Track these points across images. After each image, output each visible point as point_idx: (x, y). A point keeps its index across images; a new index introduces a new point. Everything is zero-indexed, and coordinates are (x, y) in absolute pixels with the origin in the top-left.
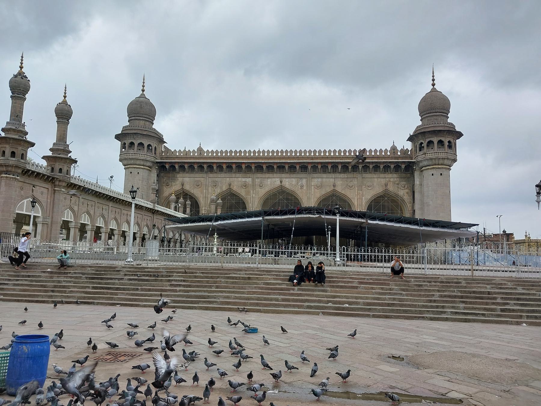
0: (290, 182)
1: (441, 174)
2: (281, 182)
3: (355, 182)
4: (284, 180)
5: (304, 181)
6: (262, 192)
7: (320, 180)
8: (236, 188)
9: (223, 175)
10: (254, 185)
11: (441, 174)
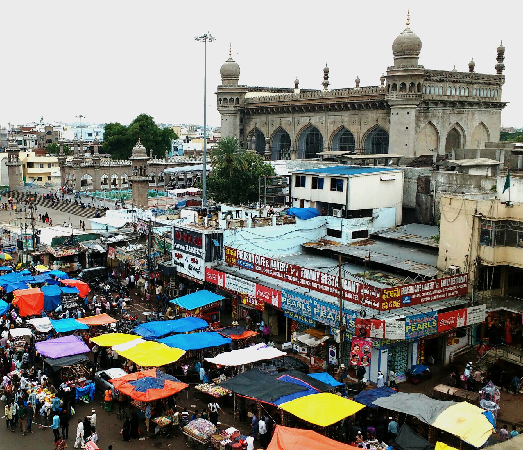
0: (315, 120)
1: (397, 114)
2: (310, 120)
3: (357, 118)
4: (312, 118)
5: (324, 118)
6: (298, 128)
7: (332, 117)
8: (283, 126)
9: (276, 116)
10: (294, 124)
11: (397, 114)
